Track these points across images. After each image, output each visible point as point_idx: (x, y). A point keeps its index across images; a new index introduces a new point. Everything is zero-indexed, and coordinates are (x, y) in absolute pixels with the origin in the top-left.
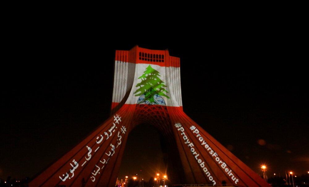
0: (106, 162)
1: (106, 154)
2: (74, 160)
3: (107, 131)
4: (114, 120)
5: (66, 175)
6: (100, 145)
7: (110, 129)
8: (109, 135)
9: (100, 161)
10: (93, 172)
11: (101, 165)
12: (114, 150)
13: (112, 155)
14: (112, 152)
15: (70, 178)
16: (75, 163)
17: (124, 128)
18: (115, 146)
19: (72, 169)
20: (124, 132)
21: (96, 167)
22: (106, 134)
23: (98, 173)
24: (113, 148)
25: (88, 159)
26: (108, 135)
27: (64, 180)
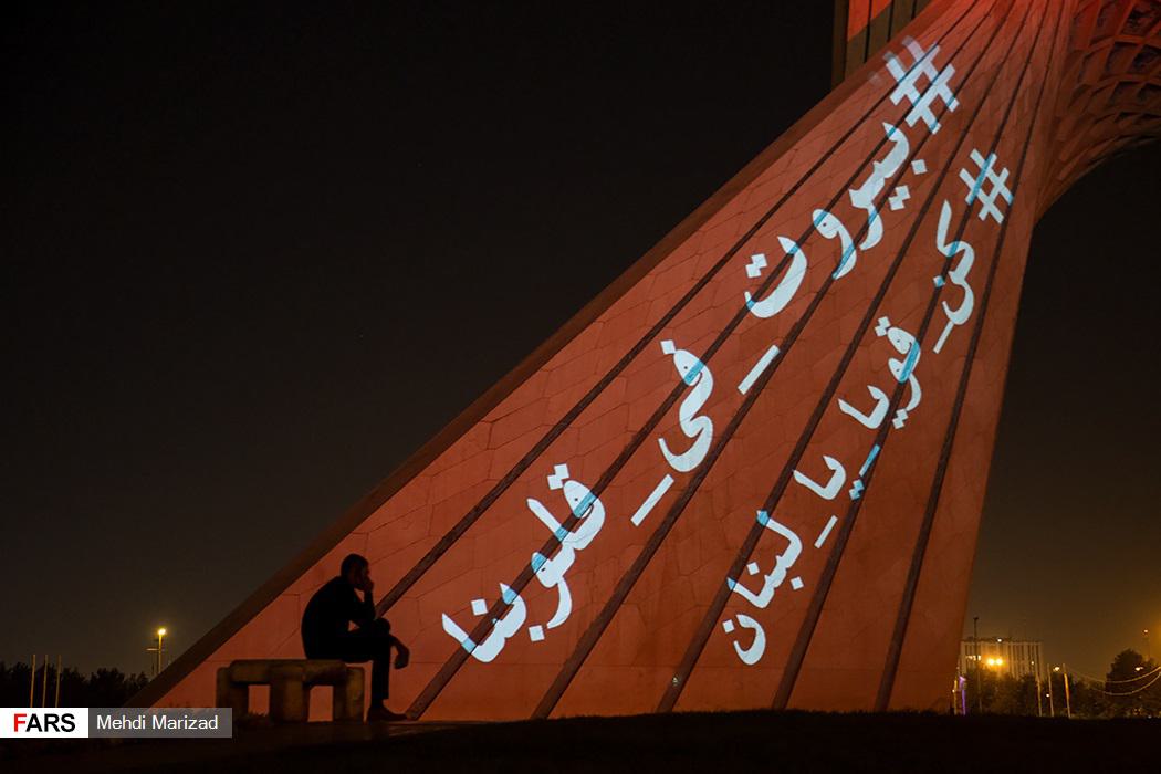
0: (848, 485)
1: (845, 407)
2: (562, 471)
3: (837, 203)
4: (896, 98)
5: (500, 610)
6: (790, 331)
7: (857, 179)
8: (859, 237)
9: (799, 477)
10: (738, 573)
11: (808, 515)
12: (914, 373)
13: (898, 423)
14: (899, 394)
15: (536, 634)
16: (577, 494)
17: (989, 173)
18: (920, 340)
19: (551, 547)
20: (989, 209)
21: (759, 529)
22: (830, 226)
23: (787, 582)
24: (901, 357)
25: (687, 462)
26: (847, 241)
27: (487, 652)
